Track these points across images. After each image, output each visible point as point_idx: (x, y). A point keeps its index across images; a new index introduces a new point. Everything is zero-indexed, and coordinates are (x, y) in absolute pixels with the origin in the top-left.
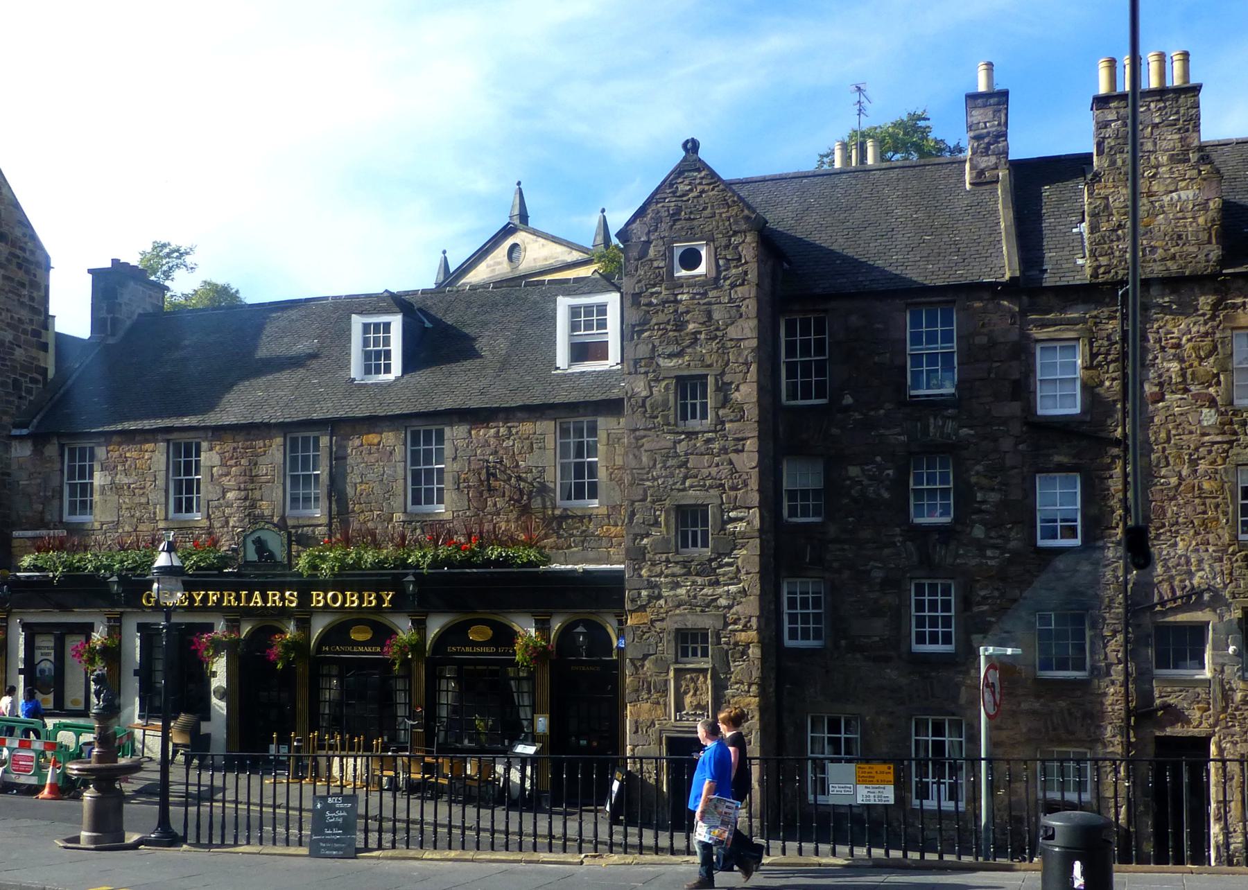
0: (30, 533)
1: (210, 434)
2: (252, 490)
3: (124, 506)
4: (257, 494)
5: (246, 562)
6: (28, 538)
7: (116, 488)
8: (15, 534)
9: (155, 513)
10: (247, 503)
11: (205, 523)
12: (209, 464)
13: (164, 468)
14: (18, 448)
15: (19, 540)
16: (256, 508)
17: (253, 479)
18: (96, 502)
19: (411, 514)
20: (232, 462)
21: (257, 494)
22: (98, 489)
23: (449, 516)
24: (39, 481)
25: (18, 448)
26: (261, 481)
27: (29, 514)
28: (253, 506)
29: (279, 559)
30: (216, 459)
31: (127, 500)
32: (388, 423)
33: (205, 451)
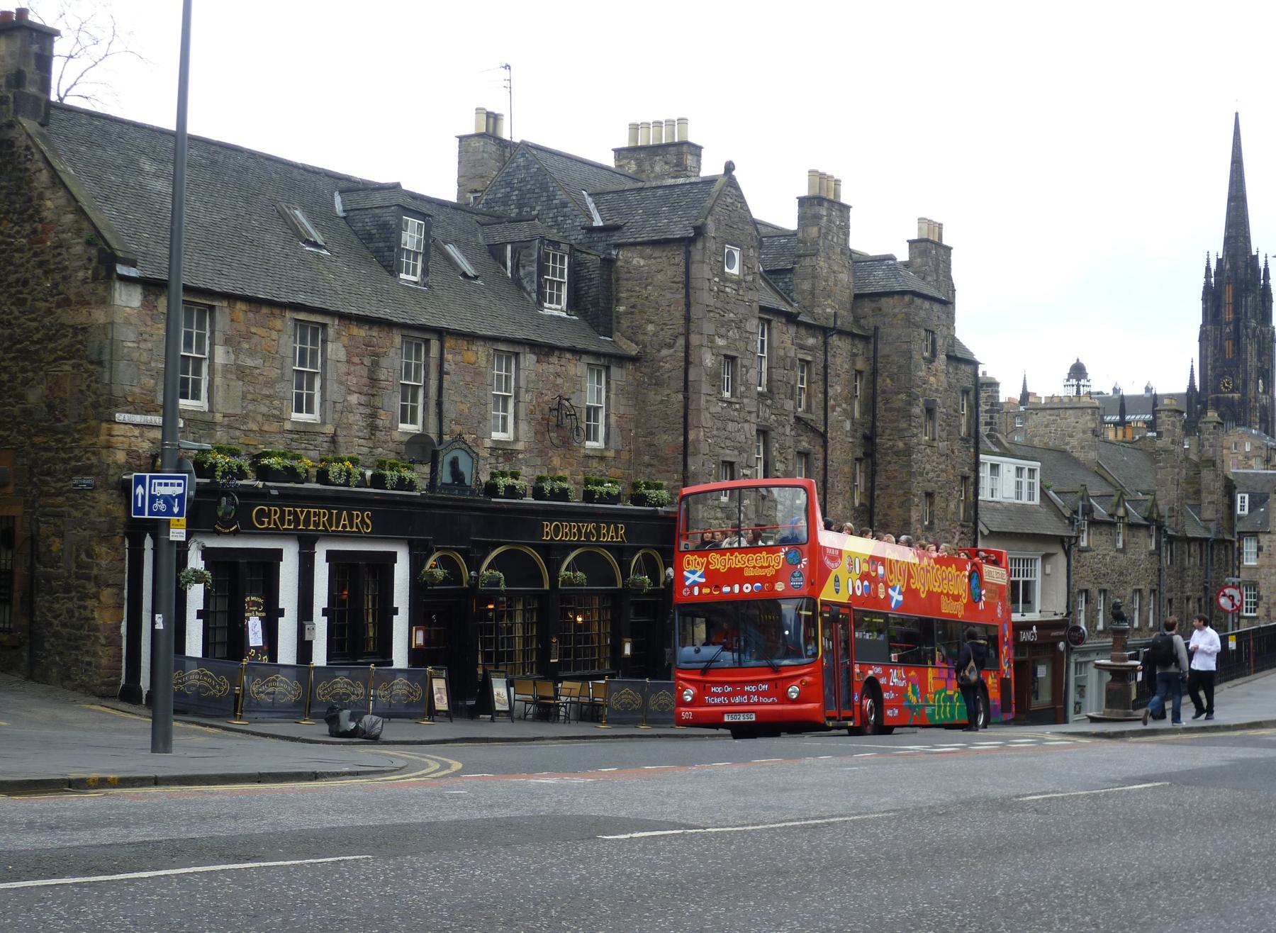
0: (138, 419)
1: (337, 322)
2: (373, 395)
3: (249, 397)
4: (377, 402)
5: (443, 484)
6: (135, 425)
7: (241, 372)
8: (120, 417)
9: (281, 410)
10: (368, 411)
11: (329, 429)
12: (334, 357)
13: (292, 356)
14: (124, 298)
15: (122, 426)
16: (376, 417)
17: (373, 380)
18: (217, 386)
19: (494, 441)
20: (356, 360)
21: (377, 402)
22: (220, 368)
23: (520, 446)
24: (149, 345)
25: (123, 292)
26: (381, 386)
27: (137, 390)
28: (373, 416)
29: (467, 481)
30: (342, 355)
31: (251, 389)
32: (482, 343)
33: (332, 342)
